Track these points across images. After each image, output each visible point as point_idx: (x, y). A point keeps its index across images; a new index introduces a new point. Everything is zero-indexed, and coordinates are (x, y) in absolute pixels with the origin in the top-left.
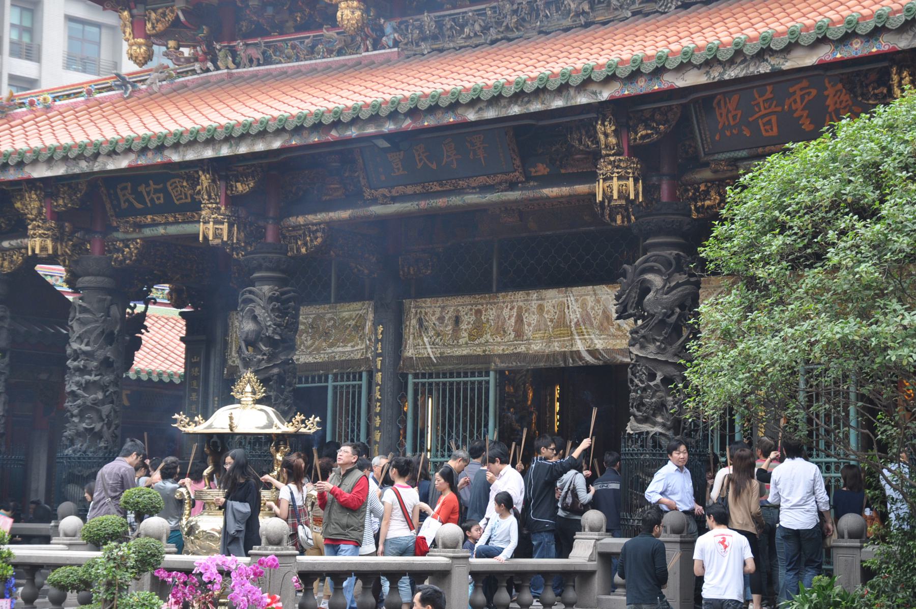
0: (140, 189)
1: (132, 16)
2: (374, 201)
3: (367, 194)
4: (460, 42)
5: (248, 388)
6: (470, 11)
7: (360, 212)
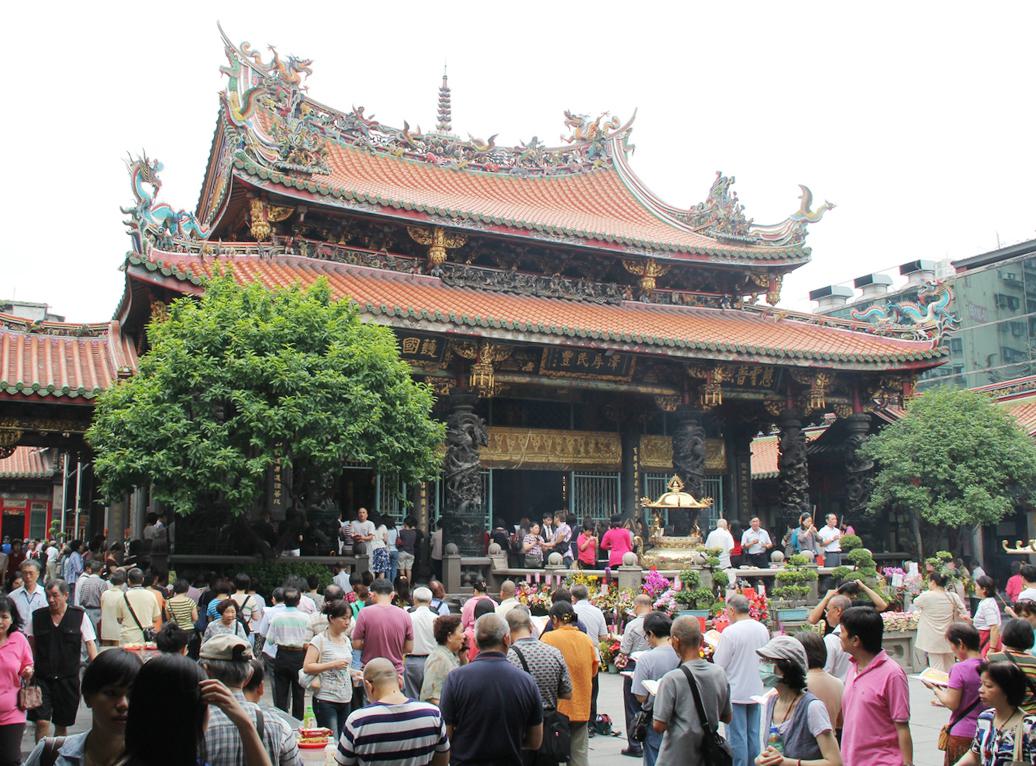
2: (545, 375)
3: (541, 373)
5: (675, 484)
7: (536, 380)
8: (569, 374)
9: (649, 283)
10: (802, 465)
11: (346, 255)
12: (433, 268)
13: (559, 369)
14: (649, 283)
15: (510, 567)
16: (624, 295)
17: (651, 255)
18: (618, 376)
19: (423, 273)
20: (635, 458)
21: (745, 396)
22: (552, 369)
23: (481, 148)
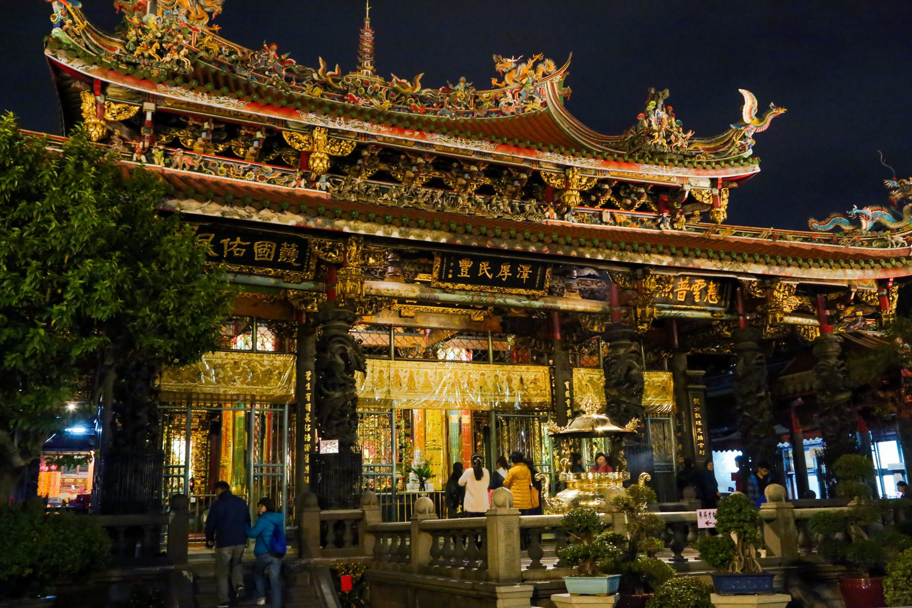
0: (222, 241)
1: (96, 102)
8: (469, 287)
10: (763, 394)
13: (456, 280)
15: (384, 520)
16: (547, 214)
18: (531, 288)
19: (306, 186)
20: (567, 394)
21: (688, 314)
22: (447, 280)
23: (406, 91)
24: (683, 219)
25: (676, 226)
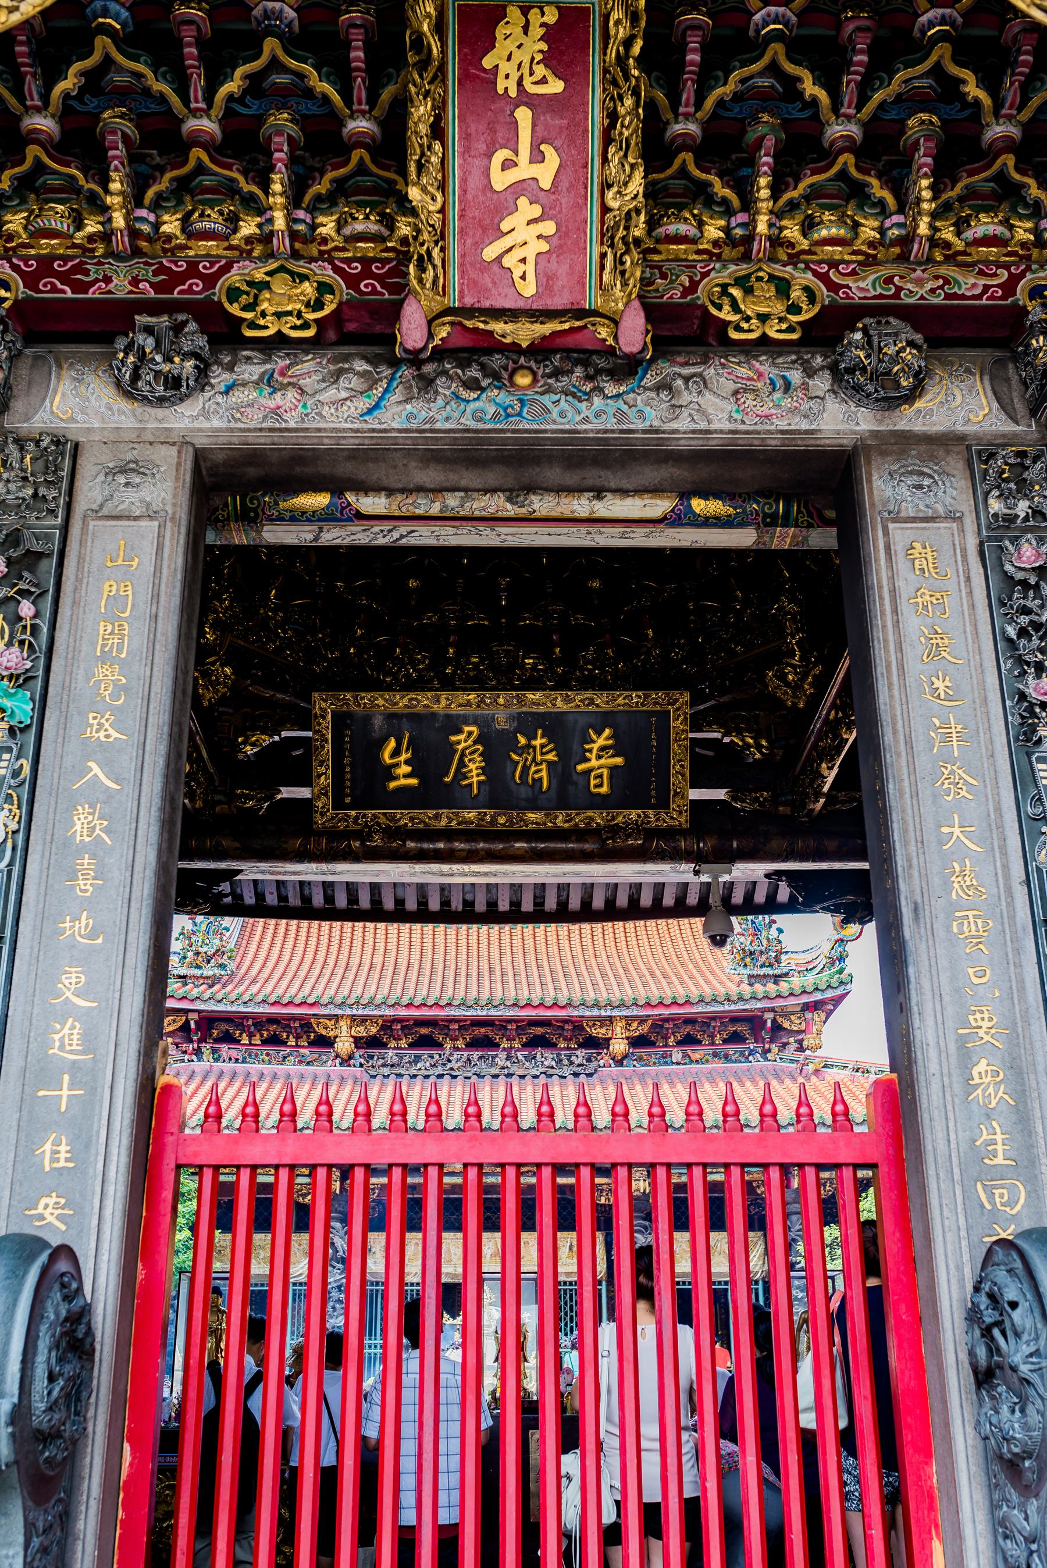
4: (412, 1071)
6: (425, 1053)
9: (619, 1046)
11: (257, 1055)
12: (350, 1057)
14: (619, 1046)
16: (601, 1062)
17: (609, 1013)
24: (775, 1048)
25: (769, 1056)
